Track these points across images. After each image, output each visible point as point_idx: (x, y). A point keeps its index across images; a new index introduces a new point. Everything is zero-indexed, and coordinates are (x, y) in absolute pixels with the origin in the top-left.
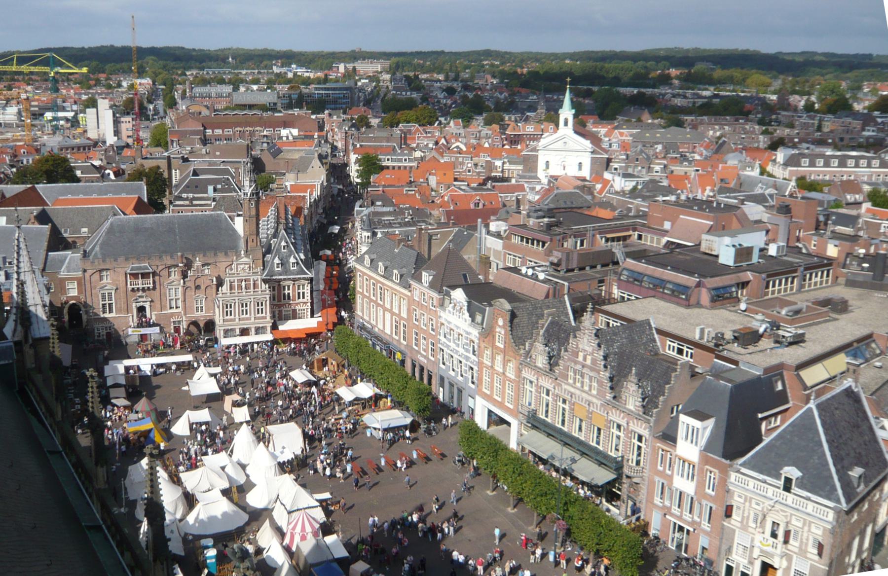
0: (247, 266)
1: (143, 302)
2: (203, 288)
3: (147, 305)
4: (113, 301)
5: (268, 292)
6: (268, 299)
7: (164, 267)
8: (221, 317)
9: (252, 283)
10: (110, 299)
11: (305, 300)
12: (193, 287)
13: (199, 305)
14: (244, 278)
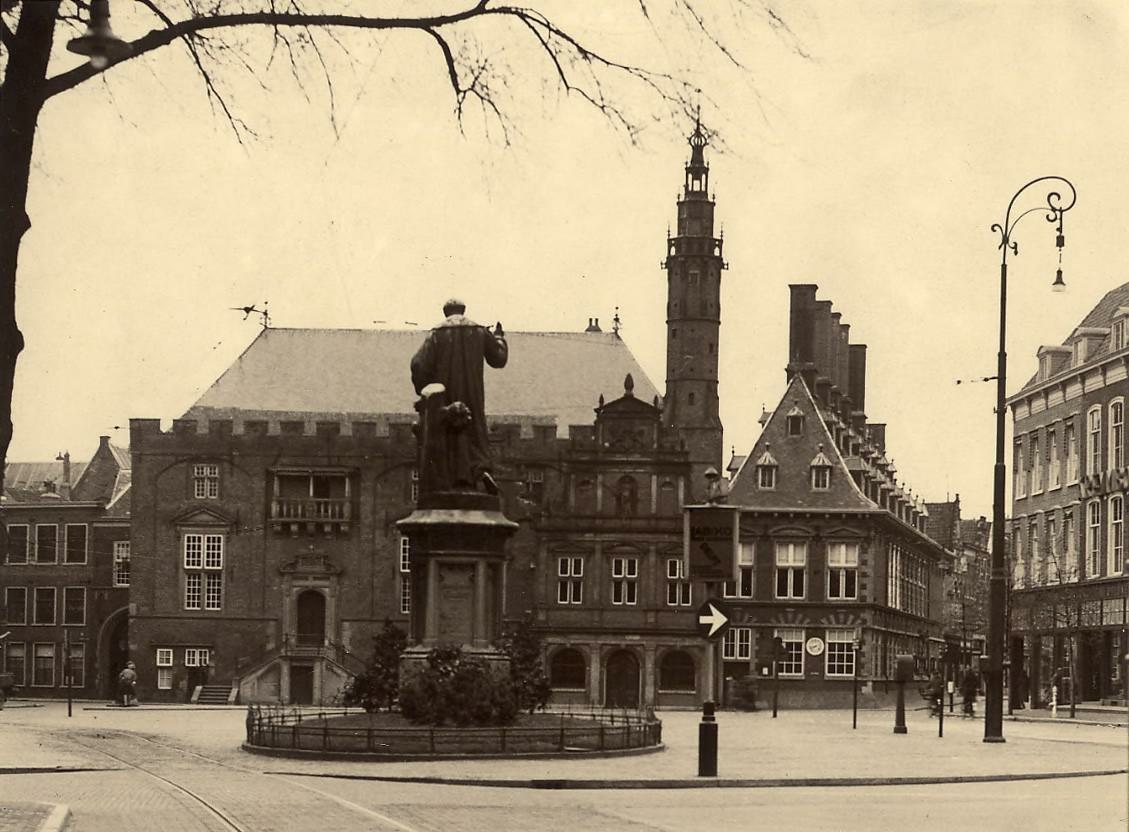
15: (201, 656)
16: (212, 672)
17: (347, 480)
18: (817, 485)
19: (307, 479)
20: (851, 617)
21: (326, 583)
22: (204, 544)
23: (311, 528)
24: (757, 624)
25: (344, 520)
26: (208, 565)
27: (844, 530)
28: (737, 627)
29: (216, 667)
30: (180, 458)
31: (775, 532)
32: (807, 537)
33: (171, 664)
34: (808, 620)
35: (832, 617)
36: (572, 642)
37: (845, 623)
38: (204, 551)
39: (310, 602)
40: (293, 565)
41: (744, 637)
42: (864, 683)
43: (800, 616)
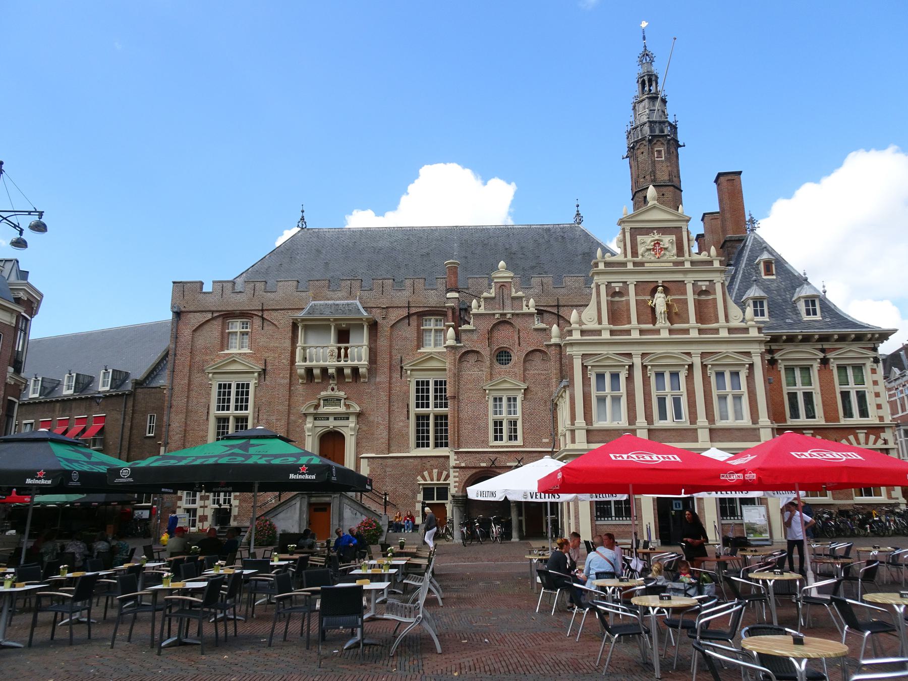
0: (667, 240)
1: (338, 417)
2: (517, 356)
3: (349, 429)
4: (249, 412)
5: (754, 333)
6: (757, 360)
7: (405, 313)
8: (580, 421)
9: (690, 298)
10: (242, 404)
11: (872, 419)
12: (486, 352)
13: (504, 416)
14: (660, 278)
15: (225, 496)
16: (235, 512)
17: (365, 327)
18: (808, 313)
19: (329, 327)
20: (872, 438)
22: (233, 390)
23: (331, 371)
25: (362, 362)
26: (236, 409)
27: (850, 351)
29: (240, 507)
30: (216, 314)
32: (815, 359)
35: (851, 438)
37: (867, 443)
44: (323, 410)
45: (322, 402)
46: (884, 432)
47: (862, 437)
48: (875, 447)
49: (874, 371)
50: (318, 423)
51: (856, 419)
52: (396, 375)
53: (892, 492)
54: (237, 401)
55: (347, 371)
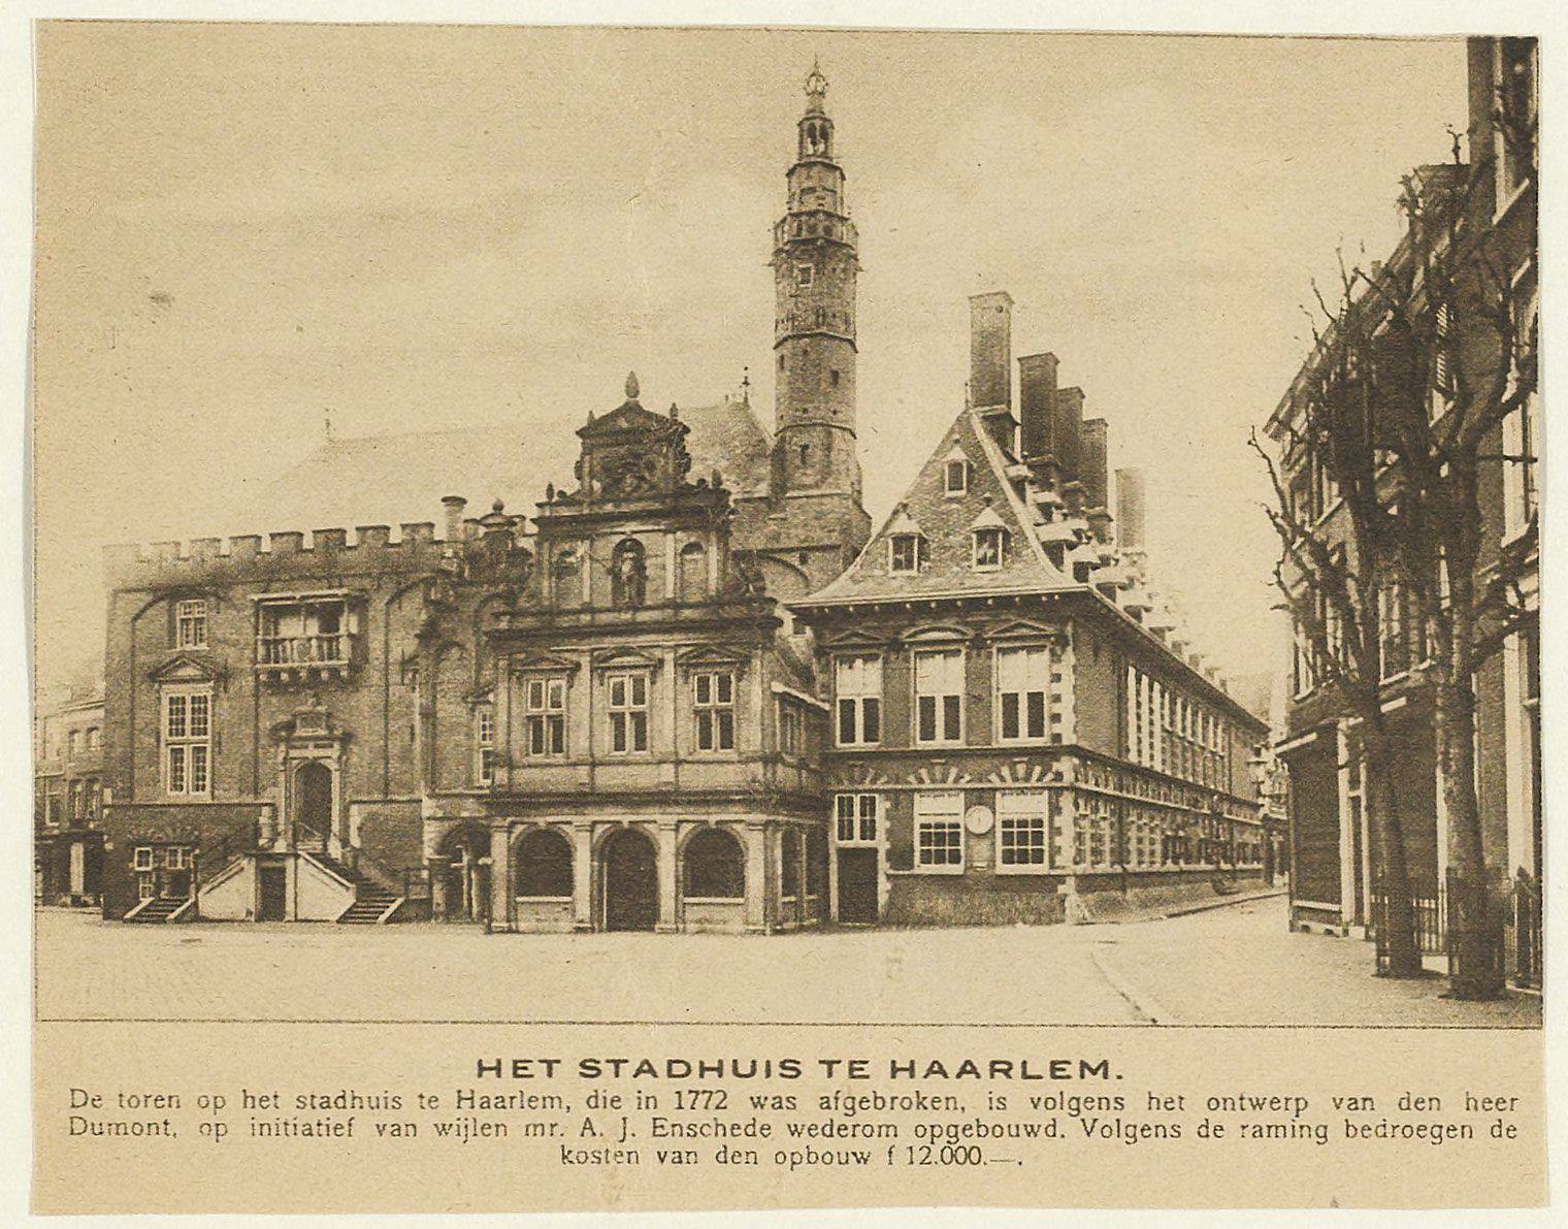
20: (1038, 769)
21: (328, 752)
24: (890, 786)
28: (858, 792)
31: (908, 637)
33: (149, 869)
34: (967, 777)
36: (551, 819)
38: (188, 716)
39: (314, 776)
40: (290, 727)
41: (869, 806)
42: (1061, 879)
43: (954, 772)
44: (300, 732)
45: (298, 722)
46: (1058, 760)
47: (1021, 769)
48: (1039, 784)
49: (1056, 658)
50: (293, 753)
51: (1024, 739)
52: (395, 678)
53: (1057, 858)
54: (193, 723)
55: (325, 675)
